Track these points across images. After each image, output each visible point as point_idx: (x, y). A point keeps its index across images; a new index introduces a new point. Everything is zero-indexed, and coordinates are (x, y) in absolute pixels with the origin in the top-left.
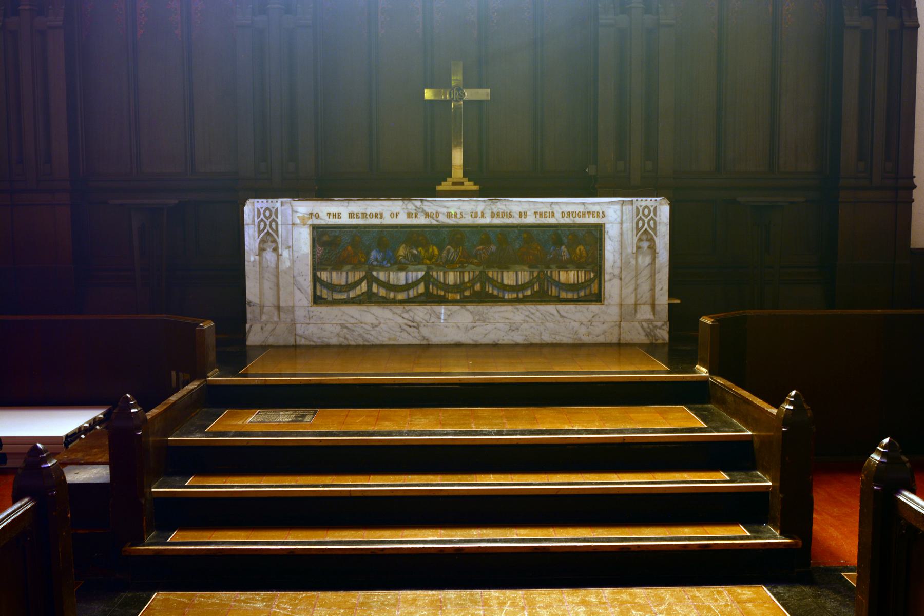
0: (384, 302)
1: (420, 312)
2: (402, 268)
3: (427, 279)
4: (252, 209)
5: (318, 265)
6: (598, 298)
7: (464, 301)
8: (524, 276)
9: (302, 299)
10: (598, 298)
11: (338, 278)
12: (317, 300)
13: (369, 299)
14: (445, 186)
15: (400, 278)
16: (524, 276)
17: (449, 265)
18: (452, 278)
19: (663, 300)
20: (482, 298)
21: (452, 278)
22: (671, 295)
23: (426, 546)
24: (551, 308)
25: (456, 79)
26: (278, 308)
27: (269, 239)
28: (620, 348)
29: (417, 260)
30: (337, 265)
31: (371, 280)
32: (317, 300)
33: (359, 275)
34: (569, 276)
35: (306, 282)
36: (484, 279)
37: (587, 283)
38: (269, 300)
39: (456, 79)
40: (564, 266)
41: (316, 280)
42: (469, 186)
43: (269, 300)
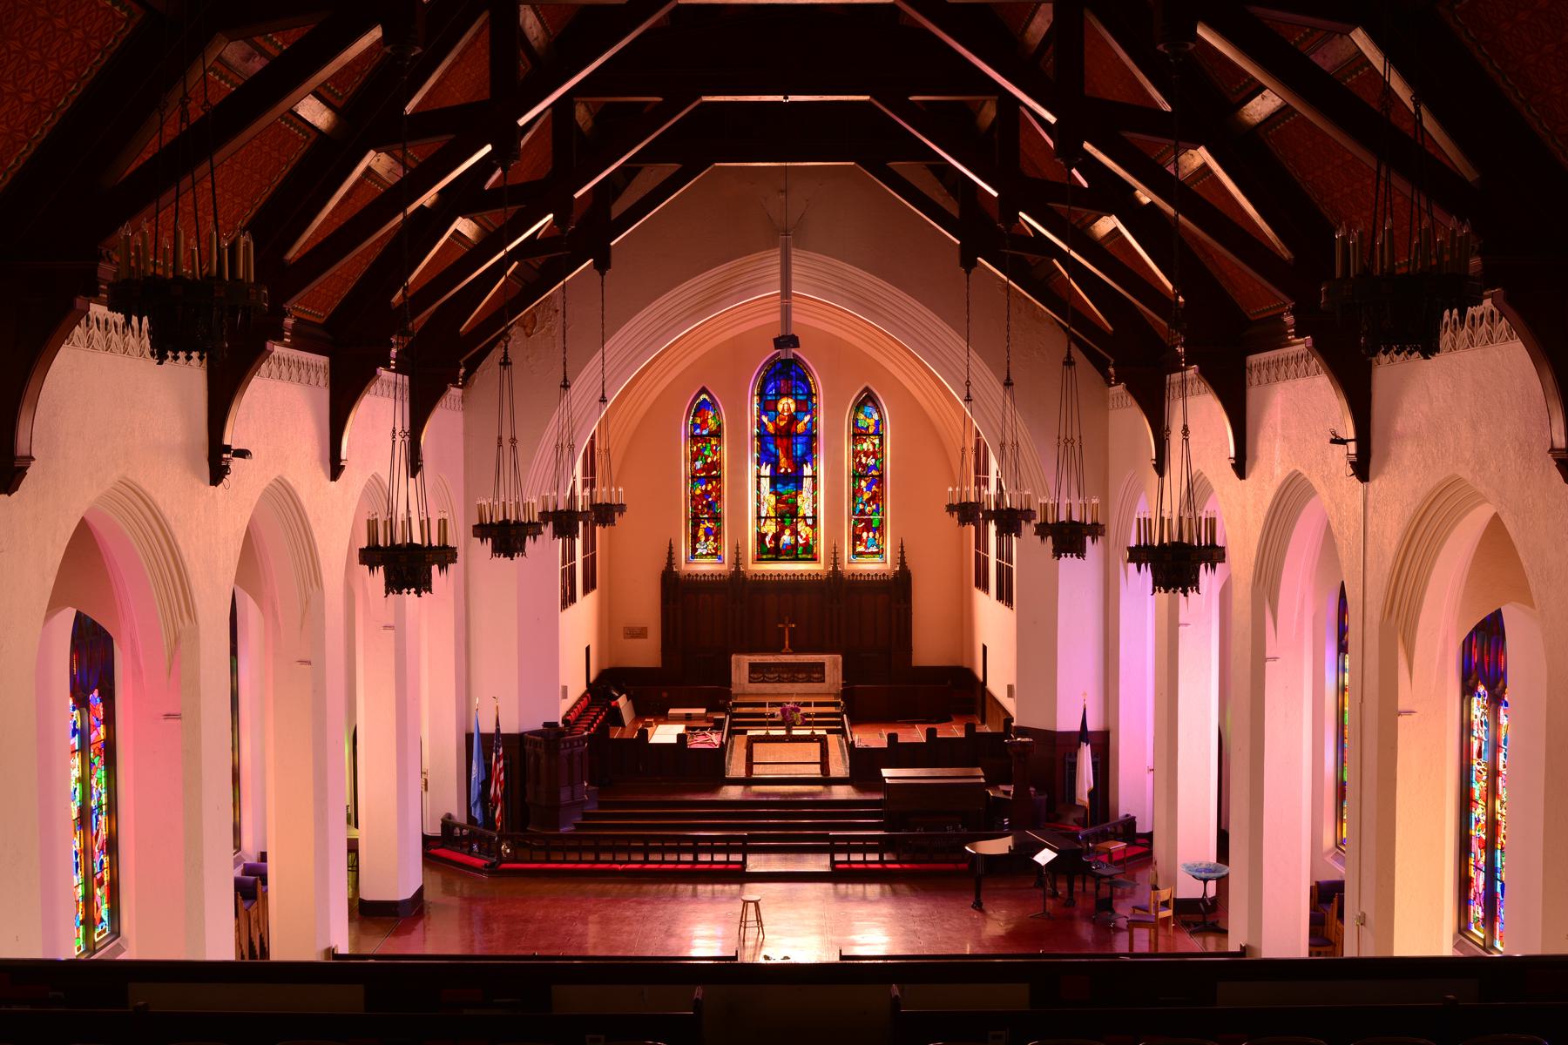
0: (768, 682)
1: (777, 685)
2: (772, 673)
3: (779, 676)
4: (734, 657)
5: (750, 674)
6: (824, 681)
7: (788, 682)
8: (804, 676)
9: (746, 681)
10: (824, 681)
11: (756, 676)
12: (750, 682)
13: (763, 682)
14: (783, 651)
15: (771, 676)
16: (804, 676)
17: (784, 673)
18: (785, 676)
19: (841, 682)
20: (793, 681)
21: (785, 676)
22: (843, 679)
23: (876, 962)
24: (811, 684)
25: (787, 622)
26: (740, 684)
27: (738, 666)
28: (829, 694)
29: (777, 672)
30: (755, 673)
31: (764, 677)
32: (750, 682)
33: (777, 675)
34: (816, 676)
35: (747, 677)
36: (794, 676)
37: (821, 678)
38: (738, 682)
39: (787, 622)
40: (815, 673)
41: (750, 677)
42: (790, 651)
43: (738, 682)
